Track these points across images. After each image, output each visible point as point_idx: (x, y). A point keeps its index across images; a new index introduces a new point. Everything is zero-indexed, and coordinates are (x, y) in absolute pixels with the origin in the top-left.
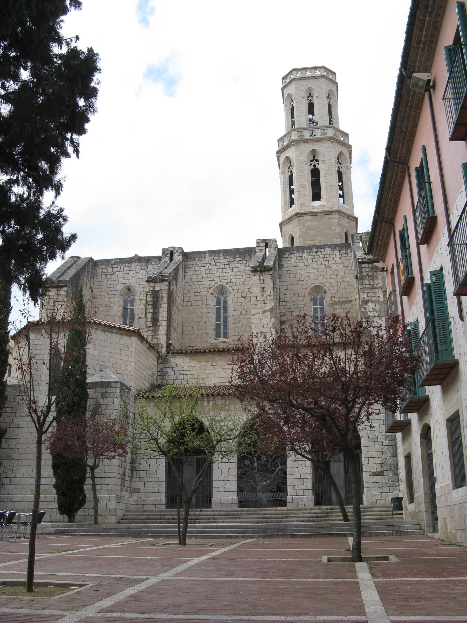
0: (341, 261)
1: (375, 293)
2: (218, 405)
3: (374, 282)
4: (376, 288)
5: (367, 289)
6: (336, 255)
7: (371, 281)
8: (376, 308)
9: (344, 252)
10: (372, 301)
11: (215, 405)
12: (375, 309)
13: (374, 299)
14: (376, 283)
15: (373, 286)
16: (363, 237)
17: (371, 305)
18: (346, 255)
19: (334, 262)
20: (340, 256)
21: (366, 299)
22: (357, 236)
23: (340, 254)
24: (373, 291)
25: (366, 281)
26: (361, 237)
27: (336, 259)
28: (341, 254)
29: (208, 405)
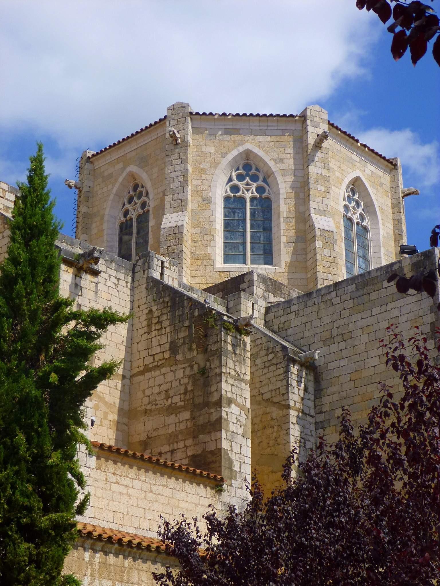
0: (115, 292)
1: (241, 389)
2: (110, 565)
3: (241, 369)
4: (242, 380)
5: (232, 377)
6: (110, 276)
7: (237, 364)
8: (241, 418)
9: (122, 276)
10: (238, 405)
11: (103, 564)
12: (238, 420)
13: (239, 400)
14: (243, 372)
15: (239, 375)
16: (166, 264)
17: (234, 408)
18: (124, 284)
19: (105, 288)
20: (115, 281)
21: (229, 395)
22: (158, 260)
23: (116, 278)
24: (238, 383)
25: (231, 361)
26: (163, 263)
27: (109, 283)
28: (118, 279)
29: (91, 563)
